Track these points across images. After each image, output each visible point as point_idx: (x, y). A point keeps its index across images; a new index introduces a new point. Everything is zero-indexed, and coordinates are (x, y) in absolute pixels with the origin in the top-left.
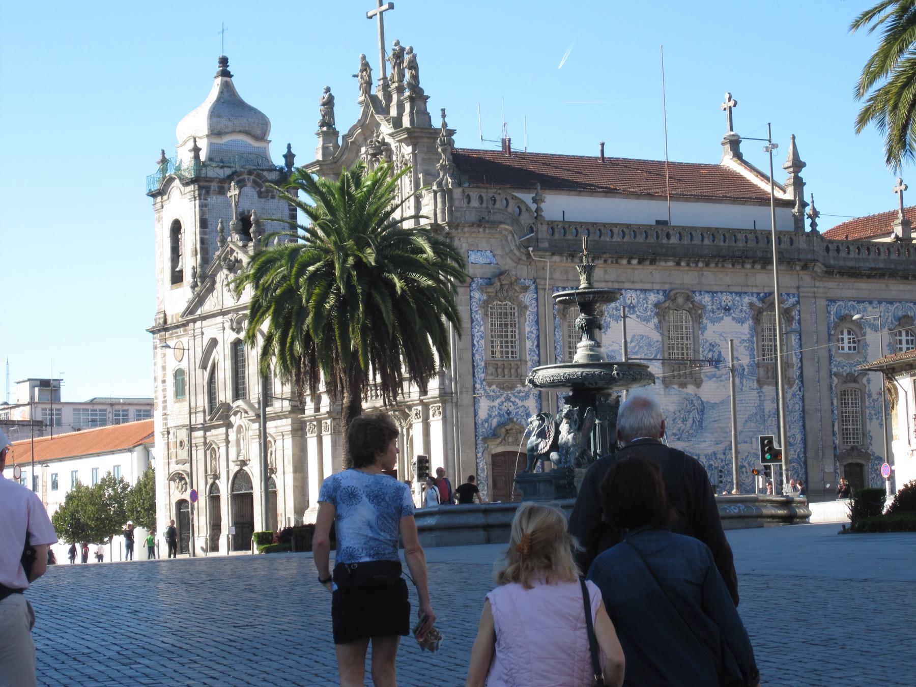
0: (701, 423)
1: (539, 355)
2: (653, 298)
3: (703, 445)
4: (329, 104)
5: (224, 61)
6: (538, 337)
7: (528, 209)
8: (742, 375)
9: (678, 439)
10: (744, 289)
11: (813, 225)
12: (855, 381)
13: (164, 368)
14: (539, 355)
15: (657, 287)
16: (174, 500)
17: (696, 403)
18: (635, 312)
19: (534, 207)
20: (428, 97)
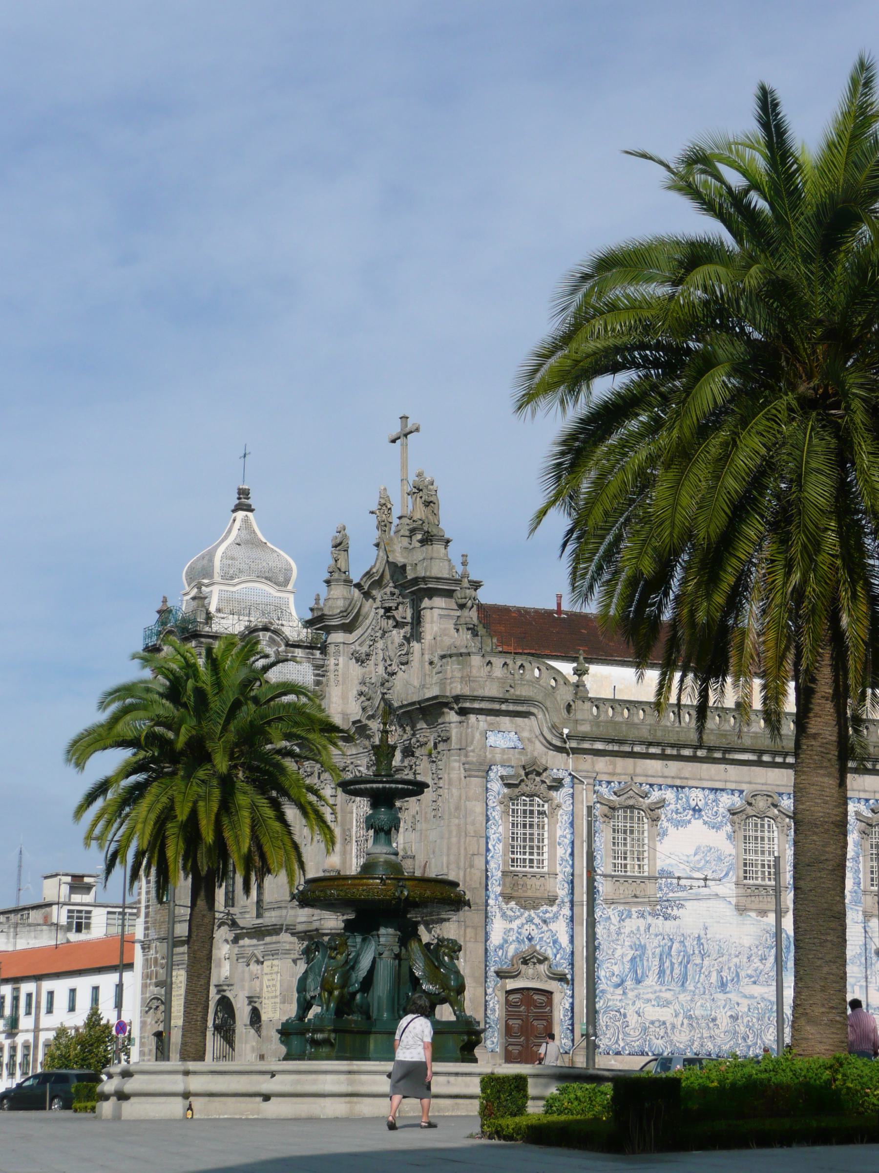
1: (573, 866)
2: (726, 800)
4: (340, 545)
5: (244, 493)
6: (573, 842)
7: (566, 682)
9: (755, 983)
14: (573, 866)
15: (732, 786)
18: (701, 817)
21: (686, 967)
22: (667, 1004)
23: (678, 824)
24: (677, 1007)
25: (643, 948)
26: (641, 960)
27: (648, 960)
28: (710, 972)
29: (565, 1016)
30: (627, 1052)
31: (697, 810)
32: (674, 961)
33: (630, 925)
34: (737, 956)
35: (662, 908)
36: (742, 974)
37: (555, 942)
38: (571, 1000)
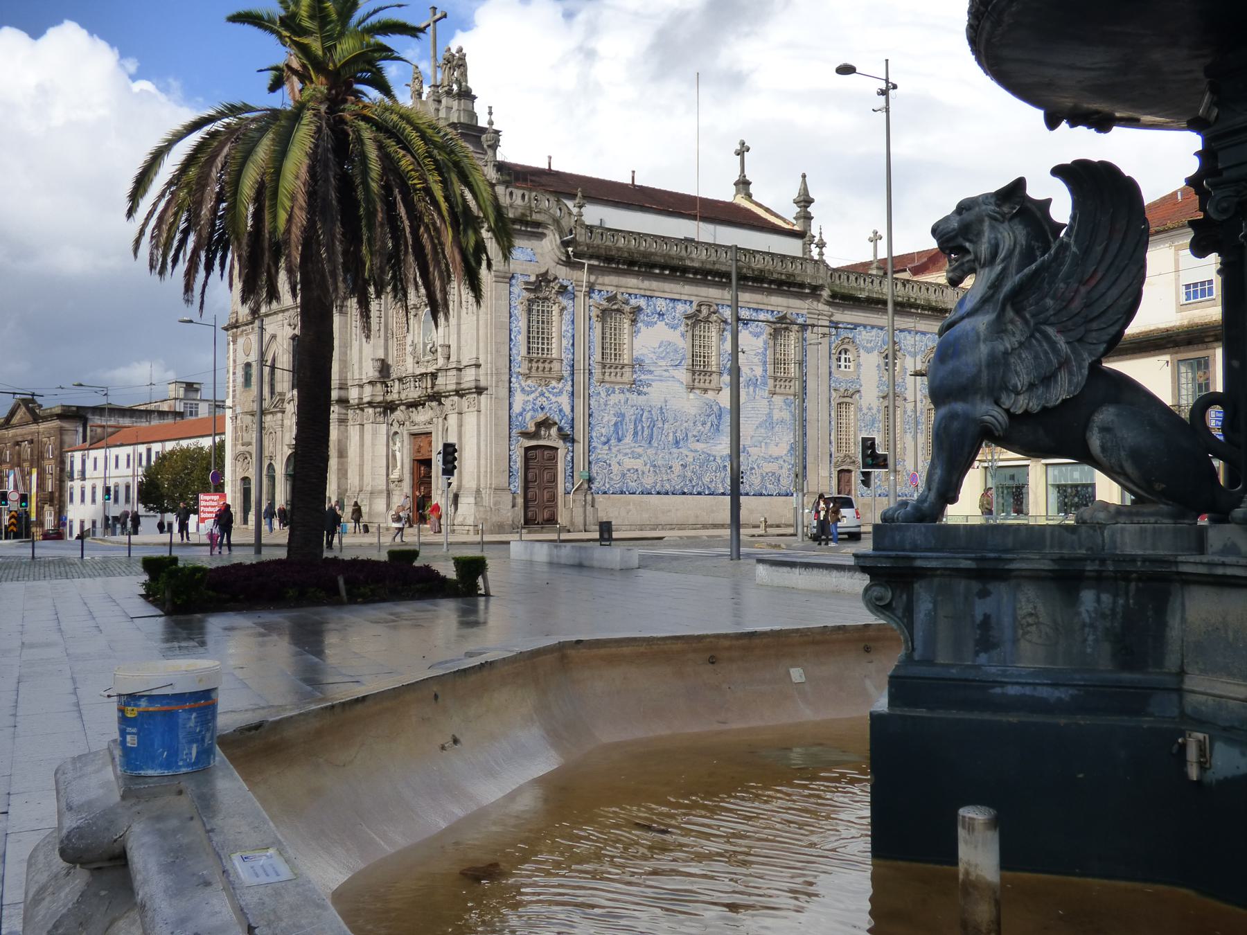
0: (718, 426)
7: (570, 213)
8: (755, 385)
10: (761, 307)
11: (821, 254)
13: (235, 361)
15: (685, 298)
16: (239, 478)
17: (715, 408)
19: (575, 211)
20: (475, 97)
22: (640, 456)
23: (649, 324)
25: (623, 415)
31: (661, 315)
33: (614, 399)
35: (635, 387)
36: (690, 435)
37: (561, 411)
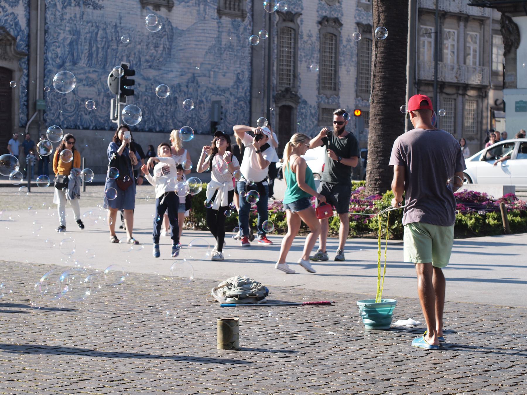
0: (170, 49)
3: (171, 75)
9: (150, 67)
12: (292, 21)
21: (106, 52)
24: (100, 86)
26: (77, 44)
27: (81, 45)
28: (122, 56)
29: (22, 93)
30: (65, 126)
32: (99, 46)
34: (140, 44)
36: (143, 59)
37: (17, 24)
38: (26, 79)
